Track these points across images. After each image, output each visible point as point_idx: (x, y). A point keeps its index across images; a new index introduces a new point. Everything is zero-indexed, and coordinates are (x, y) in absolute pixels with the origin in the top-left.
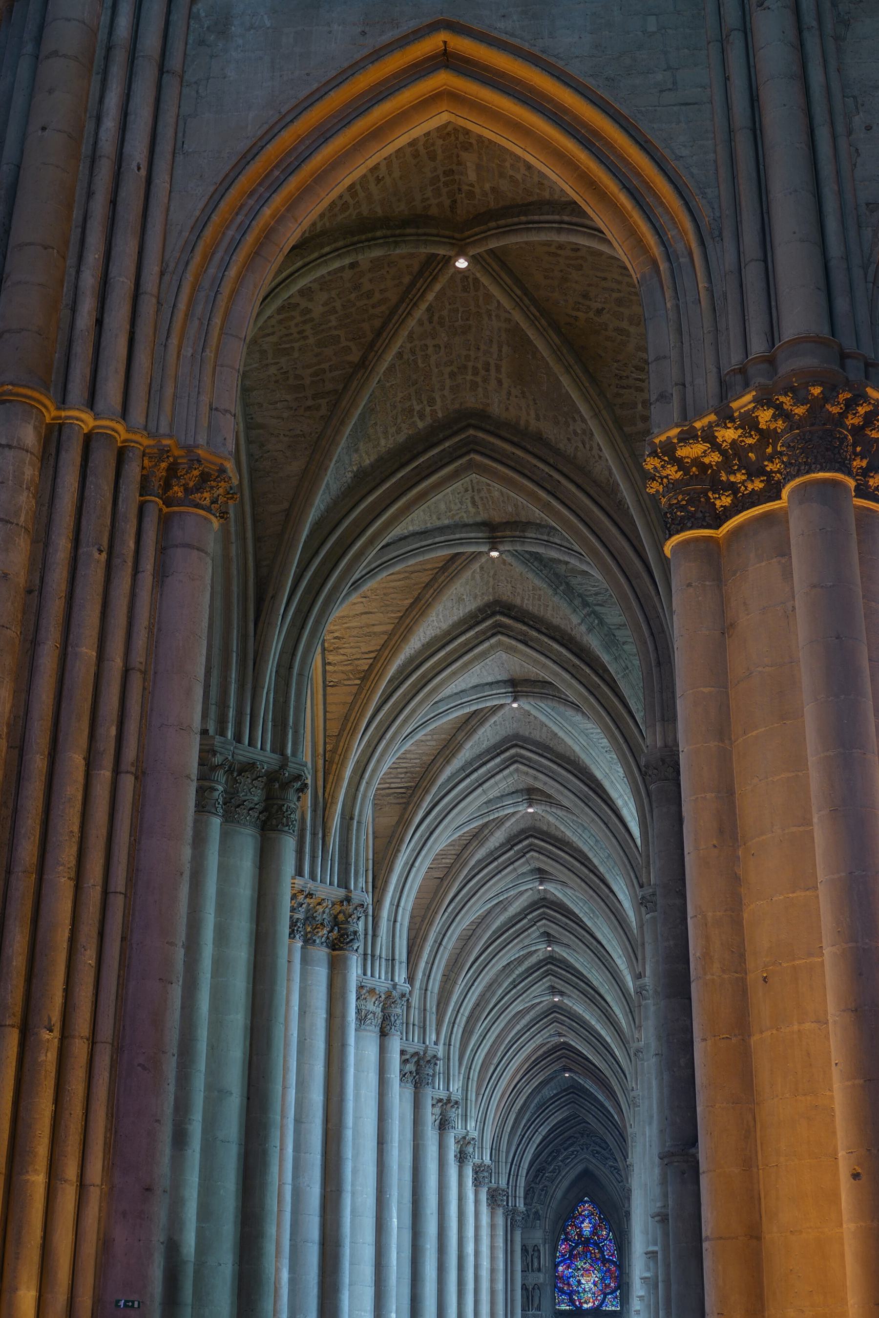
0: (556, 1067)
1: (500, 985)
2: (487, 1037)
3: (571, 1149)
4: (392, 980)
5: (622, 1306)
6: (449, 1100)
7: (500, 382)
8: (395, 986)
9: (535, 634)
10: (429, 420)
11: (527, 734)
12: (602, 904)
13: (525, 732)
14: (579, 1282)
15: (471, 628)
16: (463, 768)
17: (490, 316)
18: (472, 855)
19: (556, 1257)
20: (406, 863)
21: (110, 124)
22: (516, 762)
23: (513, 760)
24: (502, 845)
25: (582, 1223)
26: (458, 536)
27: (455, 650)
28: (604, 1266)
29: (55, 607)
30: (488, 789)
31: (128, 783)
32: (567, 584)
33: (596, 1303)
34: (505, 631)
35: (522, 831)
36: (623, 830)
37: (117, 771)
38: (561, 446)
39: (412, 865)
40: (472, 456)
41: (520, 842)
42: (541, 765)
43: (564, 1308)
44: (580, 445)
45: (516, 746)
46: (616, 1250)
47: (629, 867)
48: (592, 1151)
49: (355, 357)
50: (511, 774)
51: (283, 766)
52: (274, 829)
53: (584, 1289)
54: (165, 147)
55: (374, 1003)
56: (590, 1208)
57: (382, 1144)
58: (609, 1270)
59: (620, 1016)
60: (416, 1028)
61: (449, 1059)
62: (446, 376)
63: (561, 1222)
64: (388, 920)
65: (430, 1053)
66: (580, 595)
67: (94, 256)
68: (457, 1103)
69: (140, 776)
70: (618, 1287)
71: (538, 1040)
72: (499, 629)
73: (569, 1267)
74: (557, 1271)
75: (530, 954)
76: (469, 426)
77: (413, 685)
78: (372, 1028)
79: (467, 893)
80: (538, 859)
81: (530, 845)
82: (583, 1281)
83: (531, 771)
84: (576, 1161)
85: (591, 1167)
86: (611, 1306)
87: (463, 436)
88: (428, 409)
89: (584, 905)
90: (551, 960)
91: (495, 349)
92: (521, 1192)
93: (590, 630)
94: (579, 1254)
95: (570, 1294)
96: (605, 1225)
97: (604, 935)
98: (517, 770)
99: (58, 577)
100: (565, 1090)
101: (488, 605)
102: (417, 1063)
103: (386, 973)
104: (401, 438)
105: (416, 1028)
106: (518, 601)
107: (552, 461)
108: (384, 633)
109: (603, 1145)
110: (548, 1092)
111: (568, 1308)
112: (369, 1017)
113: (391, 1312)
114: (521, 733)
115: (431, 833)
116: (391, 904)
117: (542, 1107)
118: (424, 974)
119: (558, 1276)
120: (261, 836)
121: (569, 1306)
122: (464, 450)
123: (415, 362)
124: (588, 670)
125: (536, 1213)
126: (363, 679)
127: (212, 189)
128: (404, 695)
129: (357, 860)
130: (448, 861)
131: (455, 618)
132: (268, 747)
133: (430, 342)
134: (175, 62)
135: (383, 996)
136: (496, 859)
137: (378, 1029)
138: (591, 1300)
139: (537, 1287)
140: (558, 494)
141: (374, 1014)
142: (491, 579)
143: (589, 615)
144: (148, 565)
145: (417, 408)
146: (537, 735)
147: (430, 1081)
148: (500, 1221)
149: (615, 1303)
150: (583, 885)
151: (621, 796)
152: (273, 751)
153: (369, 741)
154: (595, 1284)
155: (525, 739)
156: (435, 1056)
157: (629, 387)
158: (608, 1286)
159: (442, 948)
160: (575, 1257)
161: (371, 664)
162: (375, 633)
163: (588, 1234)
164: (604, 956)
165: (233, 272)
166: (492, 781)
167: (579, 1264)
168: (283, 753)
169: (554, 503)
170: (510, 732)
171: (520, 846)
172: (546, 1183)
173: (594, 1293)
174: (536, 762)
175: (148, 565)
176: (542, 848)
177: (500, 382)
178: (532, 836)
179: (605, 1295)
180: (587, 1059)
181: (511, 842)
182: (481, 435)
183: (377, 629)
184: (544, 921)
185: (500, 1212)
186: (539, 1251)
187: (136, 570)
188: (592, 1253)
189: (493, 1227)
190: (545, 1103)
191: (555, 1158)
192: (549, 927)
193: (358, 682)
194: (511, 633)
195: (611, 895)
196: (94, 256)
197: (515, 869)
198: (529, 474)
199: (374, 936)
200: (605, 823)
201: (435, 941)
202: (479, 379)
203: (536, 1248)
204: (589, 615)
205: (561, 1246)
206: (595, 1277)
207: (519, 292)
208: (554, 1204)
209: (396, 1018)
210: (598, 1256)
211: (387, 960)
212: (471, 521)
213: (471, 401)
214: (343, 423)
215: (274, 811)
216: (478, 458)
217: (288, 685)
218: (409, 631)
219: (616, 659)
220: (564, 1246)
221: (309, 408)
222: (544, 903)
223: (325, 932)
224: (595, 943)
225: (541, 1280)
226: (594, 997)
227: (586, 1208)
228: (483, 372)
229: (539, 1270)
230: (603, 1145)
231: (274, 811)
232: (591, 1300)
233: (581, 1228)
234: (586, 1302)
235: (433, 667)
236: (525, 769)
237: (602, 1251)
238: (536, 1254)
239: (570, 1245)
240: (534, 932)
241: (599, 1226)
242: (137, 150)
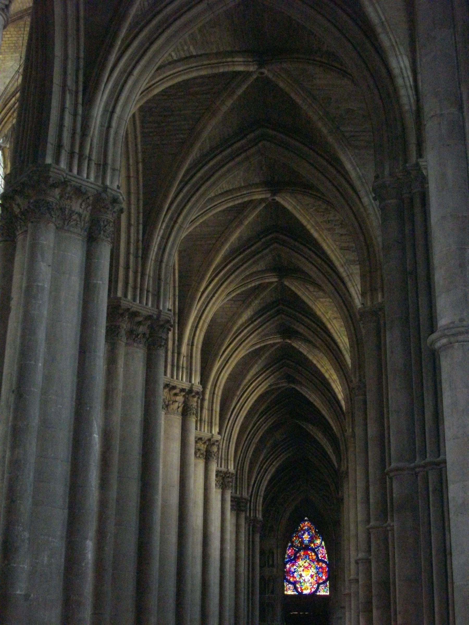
2: (230, 361)
4: (103, 183)
6: (191, 391)
14: (301, 576)
19: (284, 558)
25: (303, 535)
28: (318, 564)
33: (313, 590)
53: (304, 580)
55: (81, 205)
56: (309, 525)
57: (84, 352)
58: (321, 567)
61: (191, 357)
68: (197, 393)
73: (293, 565)
74: (285, 567)
78: (78, 230)
82: (303, 575)
86: (324, 592)
89: (311, 219)
94: (301, 556)
95: (294, 584)
97: (328, 245)
102: (151, 327)
112: (74, 217)
113: (86, 539)
118: (159, 248)
119: (287, 571)
121: (294, 591)
130: (182, 136)
141: (80, 215)
147: (163, 344)
148: (243, 522)
149: (326, 590)
154: (312, 576)
156: (168, 322)
160: (298, 558)
163: (307, 542)
167: (301, 562)
173: (311, 583)
179: (319, 584)
184: (276, 245)
186: (273, 553)
188: (309, 556)
199: (84, 135)
205: (288, 550)
206: (312, 571)
209: (105, 223)
210: (314, 557)
211: (98, 165)
220: (290, 551)
232: (309, 588)
233: (302, 538)
234: (305, 589)
237: (317, 555)
239: (295, 550)
241: (315, 537)
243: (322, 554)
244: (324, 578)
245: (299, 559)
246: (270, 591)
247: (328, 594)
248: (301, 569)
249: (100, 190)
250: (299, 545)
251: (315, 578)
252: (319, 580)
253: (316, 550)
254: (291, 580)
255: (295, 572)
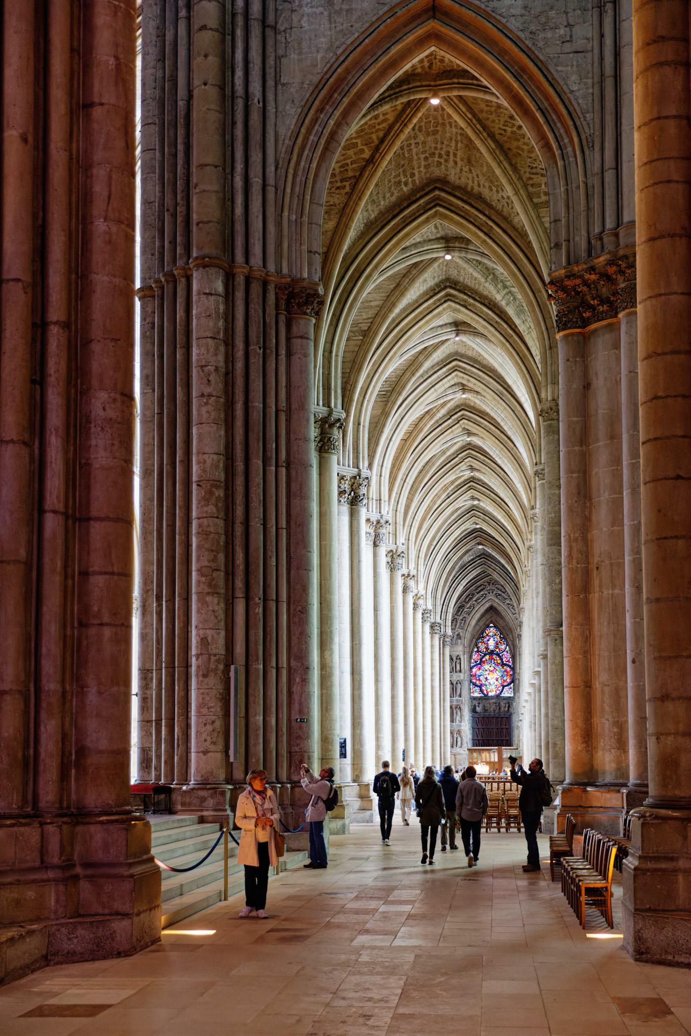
0: (473, 543)
1: (439, 497)
3: (482, 593)
5: (514, 694)
6: (409, 575)
7: (456, 163)
8: (382, 516)
9: (471, 301)
10: (410, 186)
11: (463, 352)
12: (509, 454)
13: (462, 350)
14: (486, 679)
15: (431, 297)
16: (422, 376)
17: (451, 126)
18: (425, 425)
19: (470, 663)
20: (387, 438)
21: (239, 73)
22: (456, 370)
23: (454, 369)
24: (444, 416)
26: (425, 248)
27: (421, 313)
29: (240, 382)
30: (438, 389)
31: (283, 471)
32: (494, 274)
33: (498, 692)
34: (453, 299)
35: (457, 406)
36: (524, 415)
37: (277, 466)
38: (494, 204)
39: (390, 440)
40: (438, 208)
41: (456, 413)
42: (472, 373)
44: (506, 205)
45: (456, 360)
47: (527, 439)
48: (496, 594)
49: (367, 155)
50: (453, 378)
51: (330, 413)
52: (326, 452)
54: (270, 83)
58: (506, 671)
59: (517, 516)
60: (391, 535)
62: (422, 159)
63: (474, 640)
64: (377, 475)
65: (400, 550)
66: (502, 281)
67: (239, 167)
68: (414, 576)
69: (288, 468)
70: (513, 681)
71: (463, 528)
72: (449, 298)
73: (479, 669)
75: (460, 477)
76: (436, 188)
77: (395, 336)
79: (422, 448)
80: (467, 424)
81: (463, 415)
83: (465, 376)
84: (484, 601)
85: (495, 605)
86: (507, 693)
87: (432, 196)
88: (410, 180)
90: (472, 479)
91: (453, 144)
92: (449, 623)
93: (507, 304)
95: (480, 686)
98: (456, 376)
99: (240, 365)
100: (479, 556)
101: (441, 282)
103: (376, 508)
104: (393, 199)
105: (391, 535)
106: (461, 279)
107: (487, 213)
108: (377, 306)
109: (503, 590)
110: (467, 558)
114: (460, 351)
115: (402, 419)
116: (378, 465)
117: (464, 567)
118: (395, 501)
120: (319, 456)
122: (432, 204)
123: (403, 154)
124: (505, 326)
125: (458, 635)
126: (364, 336)
127: (300, 110)
128: (389, 343)
129: (363, 450)
131: (421, 292)
132: (321, 403)
133: (413, 141)
134: (271, 19)
135: (375, 523)
136: (440, 425)
137: (372, 543)
139: (459, 682)
140: (491, 235)
142: (445, 268)
143: (507, 294)
144: (283, 352)
145: (403, 180)
146: (470, 353)
150: (497, 441)
151: (524, 395)
152: (324, 405)
153: (368, 374)
155: (462, 356)
157: (537, 174)
158: (505, 681)
159: (406, 484)
160: (484, 662)
161: (370, 327)
162: (371, 307)
164: (508, 481)
165: (314, 165)
166: (441, 383)
167: (486, 667)
168: (329, 406)
169: (489, 241)
170: (452, 351)
171: (456, 416)
172: (465, 615)
174: (469, 370)
175: (283, 352)
176: (470, 417)
177: (456, 163)
178: (463, 409)
179: (504, 687)
180: (494, 538)
181: (450, 414)
182: (443, 195)
183: (373, 304)
184: (469, 459)
185: (437, 637)
187: (277, 355)
189: (432, 646)
190: (465, 565)
191: (471, 599)
192: (473, 462)
193: (361, 338)
194: (457, 301)
195: (514, 448)
196: (239, 167)
197: (452, 431)
198: (473, 221)
200: (513, 411)
201: (402, 480)
202: (442, 161)
203: (458, 658)
204: (507, 294)
206: (497, 674)
207: (470, 116)
208: (470, 629)
210: (499, 661)
212: (434, 238)
213: (437, 172)
214: (360, 199)
215: (326, 441)
216: (441, 209)
217: (330, 363)
218: (394, 305)
219: (523, 322)
221: (338, 188)
222: (470, 446)
223: (346, 495)
224: (503, 473)
225: (462, 678)
226: (501, 504)
227: (492, 631)
228: (445, 157)
229: (460, 671)
230: (503, 590)
231: (326, 441)
233: (487, 644)
235: (407, 324)
236: (462, 375)
237: (501, 659)
238: (458, 661)
240: (463, 466)
242: (256, 87)
244: (508, 680)
246: (458, 692)
247: (512, 695)
248: (487, 673)
249: (379, 517)
251: (499, 680)
254: (478, 683)
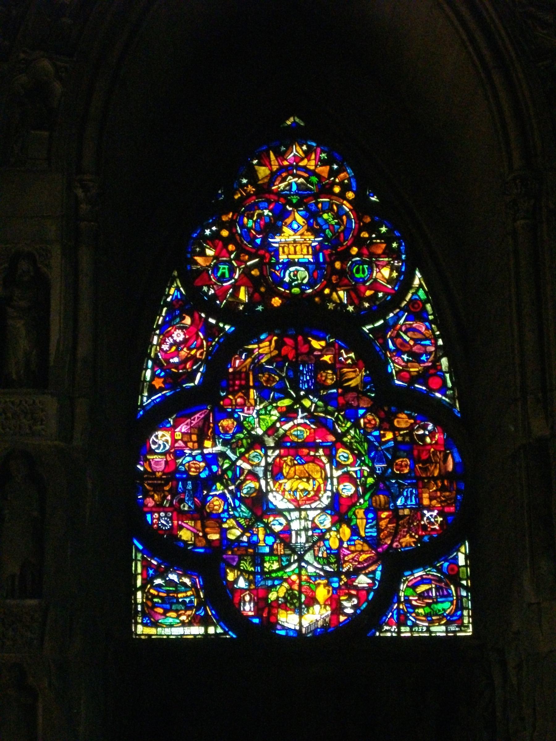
43: (177, 631)
46: (446, 351)
56: (311, 165)
94: (258, 368)
96: (388, 239)
111: (197, 630)
121: (205, 621)
138: (322, 593)
149: (446, 606)
220: (179, 336)
232: (322, 593)
243: (416, 357)
245: (246, 390)
250: (243, 296)
252: (395, 535)
253: (366, 329)
255: (213, 479)
